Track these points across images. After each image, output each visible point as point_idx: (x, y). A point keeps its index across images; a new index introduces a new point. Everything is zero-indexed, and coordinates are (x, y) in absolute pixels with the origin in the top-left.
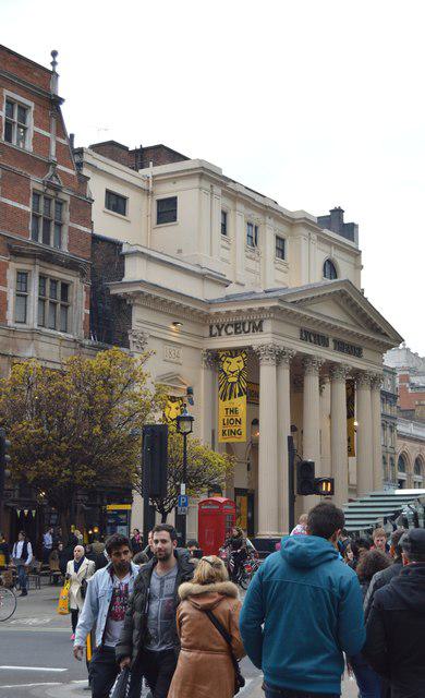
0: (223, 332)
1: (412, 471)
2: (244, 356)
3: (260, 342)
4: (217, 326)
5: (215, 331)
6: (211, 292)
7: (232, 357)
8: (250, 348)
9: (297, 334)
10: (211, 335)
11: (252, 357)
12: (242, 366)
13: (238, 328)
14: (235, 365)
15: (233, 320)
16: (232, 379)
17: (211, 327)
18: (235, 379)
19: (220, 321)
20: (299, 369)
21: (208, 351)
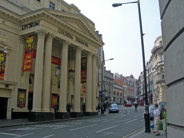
0: (26, 28)
1: (120, 96)
2: (33, 36)
3: (37, 29)
4: (25, 26)
5: (24, 27)
6: (20, 12)
7: (30, 37)
8: (34, 32)
9: (57, 30)
10: (22, 29)
11: (34, 35)
12: (32, 40)
13: (31, 25)
14: (30, 40)
15: (29, 22)
16: (29, 46)
17: (23, 27)
18: (30, 46)
19: (26, 23)
20: (58, 44)
21: (22, 36)
